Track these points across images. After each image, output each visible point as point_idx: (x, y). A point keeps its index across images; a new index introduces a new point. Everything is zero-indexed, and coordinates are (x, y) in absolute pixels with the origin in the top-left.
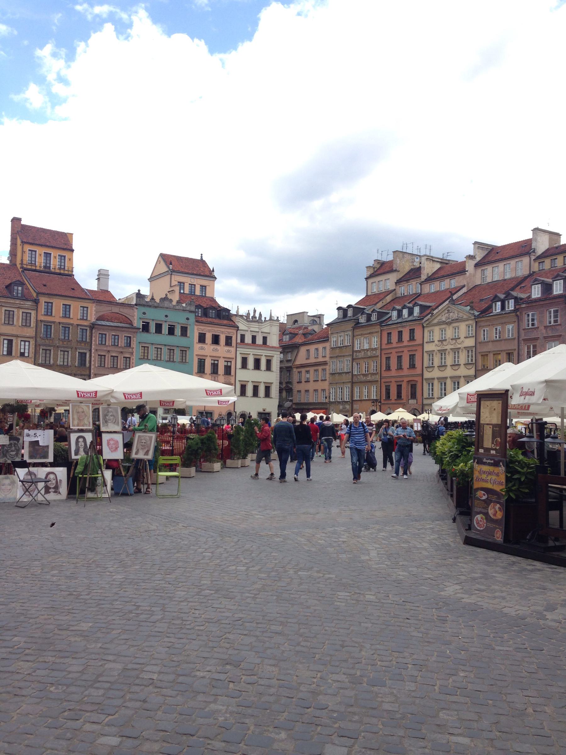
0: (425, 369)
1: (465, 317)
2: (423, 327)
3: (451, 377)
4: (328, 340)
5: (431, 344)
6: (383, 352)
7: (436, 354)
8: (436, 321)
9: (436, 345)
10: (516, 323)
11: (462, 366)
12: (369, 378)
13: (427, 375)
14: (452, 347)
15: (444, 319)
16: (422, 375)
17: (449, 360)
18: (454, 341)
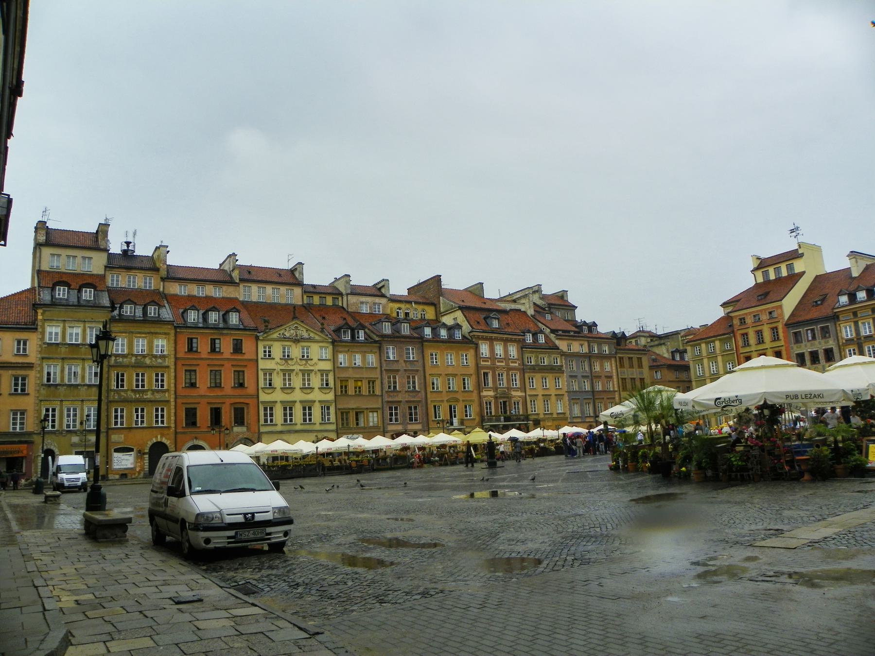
0: (260, 391)
1: (317, 338)
2: (257, 338)
3: (301, 402)
4: (36, 329)
5: (269, 361)
6: (179, 363)
7: (278, 373)
8: (275, 336)
9: (277, 363)
10: (378, 354)
11: (316, 390)
12: (149, 396)
13: (263, 397)
14: (302, 368)
15: (287, 334)
16: (258, 397)
17: (297, 382)
18: (304, 362)
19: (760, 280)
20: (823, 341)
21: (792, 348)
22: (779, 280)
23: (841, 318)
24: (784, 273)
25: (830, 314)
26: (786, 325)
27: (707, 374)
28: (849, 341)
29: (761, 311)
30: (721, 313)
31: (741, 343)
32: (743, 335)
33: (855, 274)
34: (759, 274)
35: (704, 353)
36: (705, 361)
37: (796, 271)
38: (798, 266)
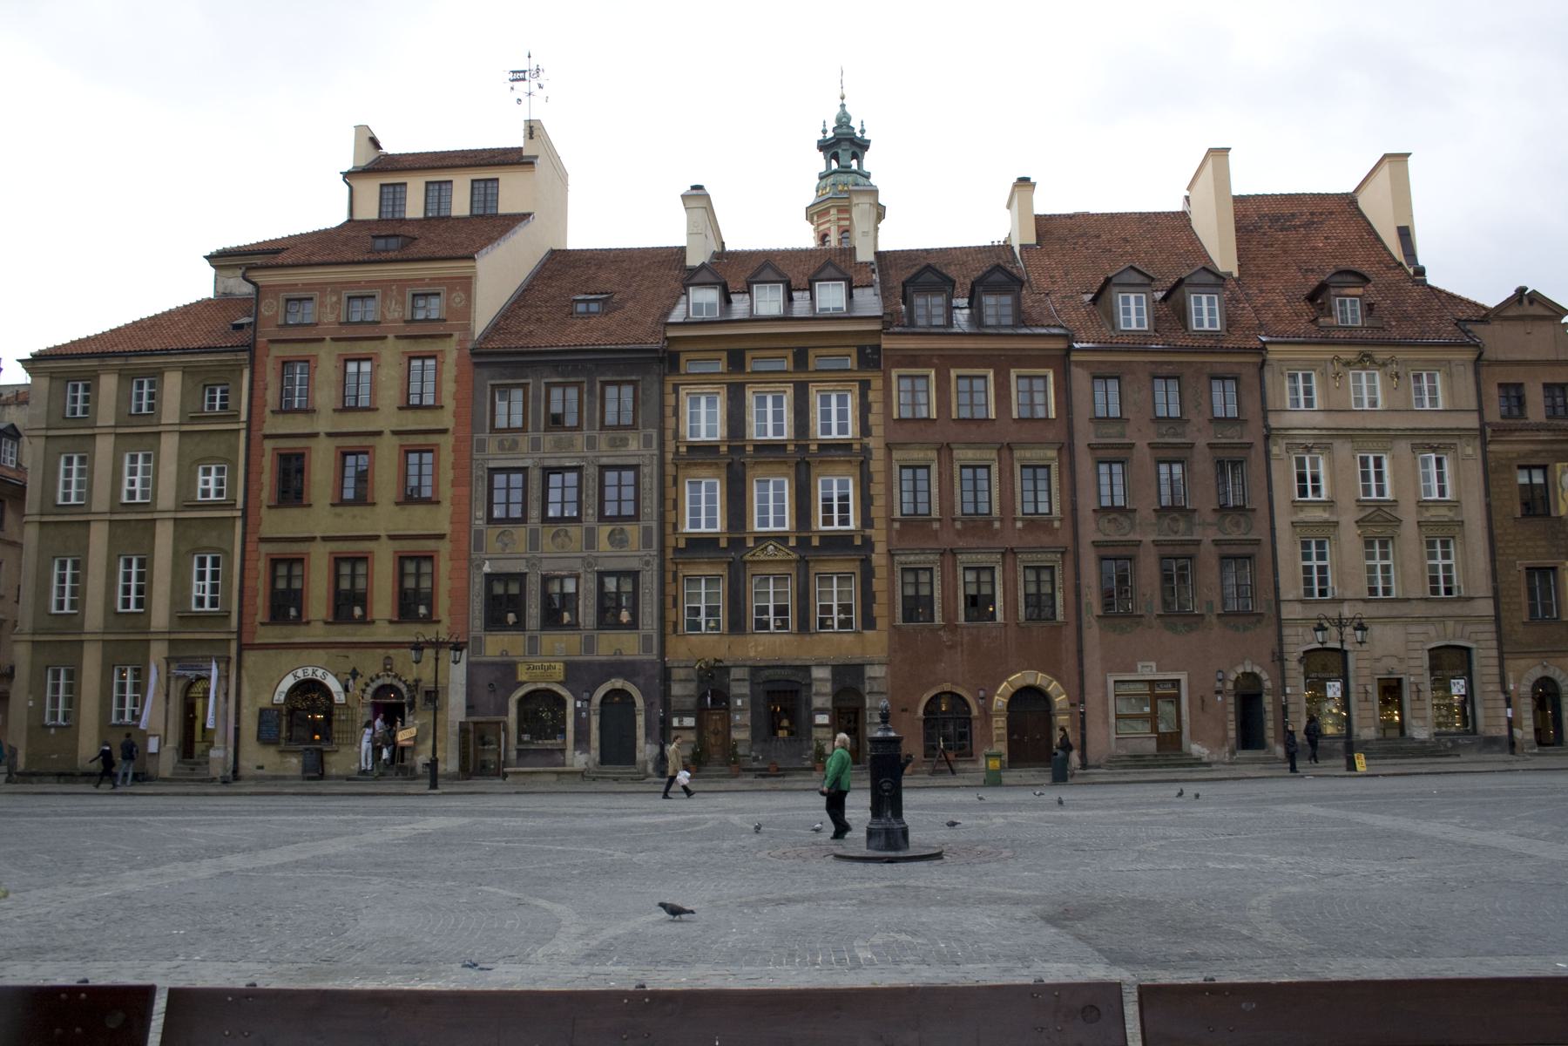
19: (369, 210)
20: (603, 440)
21: (482, 446)
22: (437, 221)
23: (685, 367)
25: (654, 343)
26: (475, 353)
27: (101, 501)
28: (702, 453)
29: (385, 285)
30: (200, 285)
31: (272, 397)
32: (286, 364)
33: (693, 260)
34: (370, 190)
35: (106, 414)
36: (104, 447)
37: (505, 207)
38: (512, 193)
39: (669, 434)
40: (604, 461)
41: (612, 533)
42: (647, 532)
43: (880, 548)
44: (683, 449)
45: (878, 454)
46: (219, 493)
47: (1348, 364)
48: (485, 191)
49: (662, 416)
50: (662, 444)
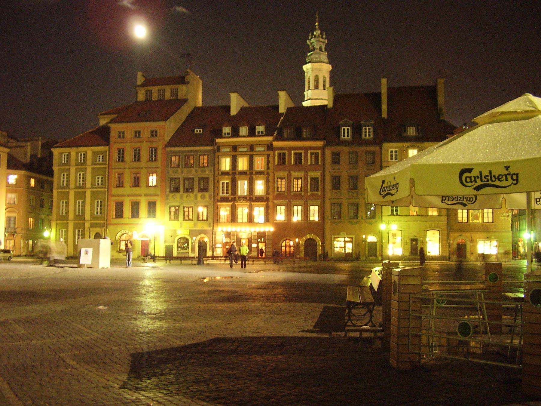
20: (199, 170)
21: (168, 172)
24: (168, 96)
28: (225, 173)
37: (181, 96)
39: (216, 169)
40: (200, 176)
41: (201, 196)
42: (210, 195)
43: (271, 200)
44: (220, 173)
45: (271, 175)
46: (102, 184)
47: (408, 147)
48: (174, 93)
49: (214, 164)
50: (214, 172)
